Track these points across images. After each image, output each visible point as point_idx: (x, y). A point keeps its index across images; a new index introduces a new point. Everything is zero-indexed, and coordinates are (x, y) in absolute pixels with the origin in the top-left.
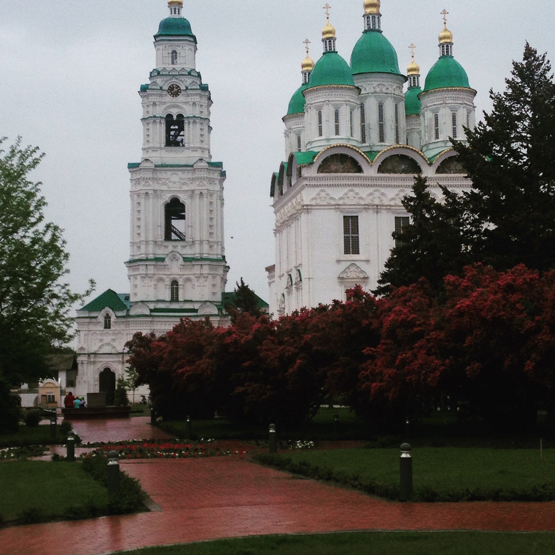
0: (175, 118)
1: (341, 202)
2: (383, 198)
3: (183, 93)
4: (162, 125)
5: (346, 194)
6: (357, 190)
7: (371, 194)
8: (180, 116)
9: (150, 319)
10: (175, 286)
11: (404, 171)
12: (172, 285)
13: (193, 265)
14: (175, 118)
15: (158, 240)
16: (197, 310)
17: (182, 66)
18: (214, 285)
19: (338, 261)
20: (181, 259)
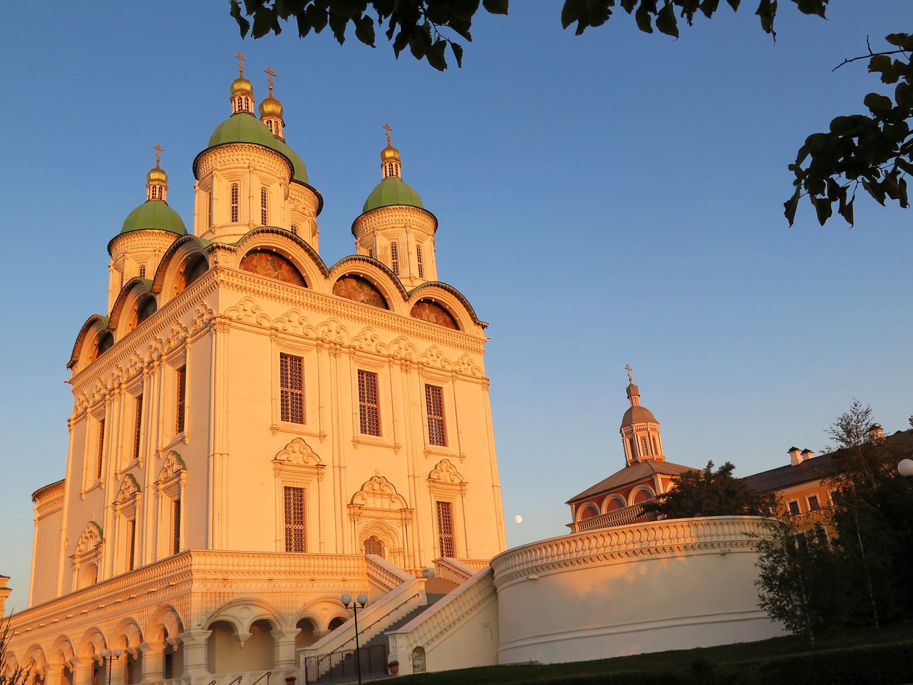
1: (280, 326)
2: (342, 333)
5: (287, 314)
6: (305, 312)
7: (324, 324)
11: (363, 301)
19: (274, 429)
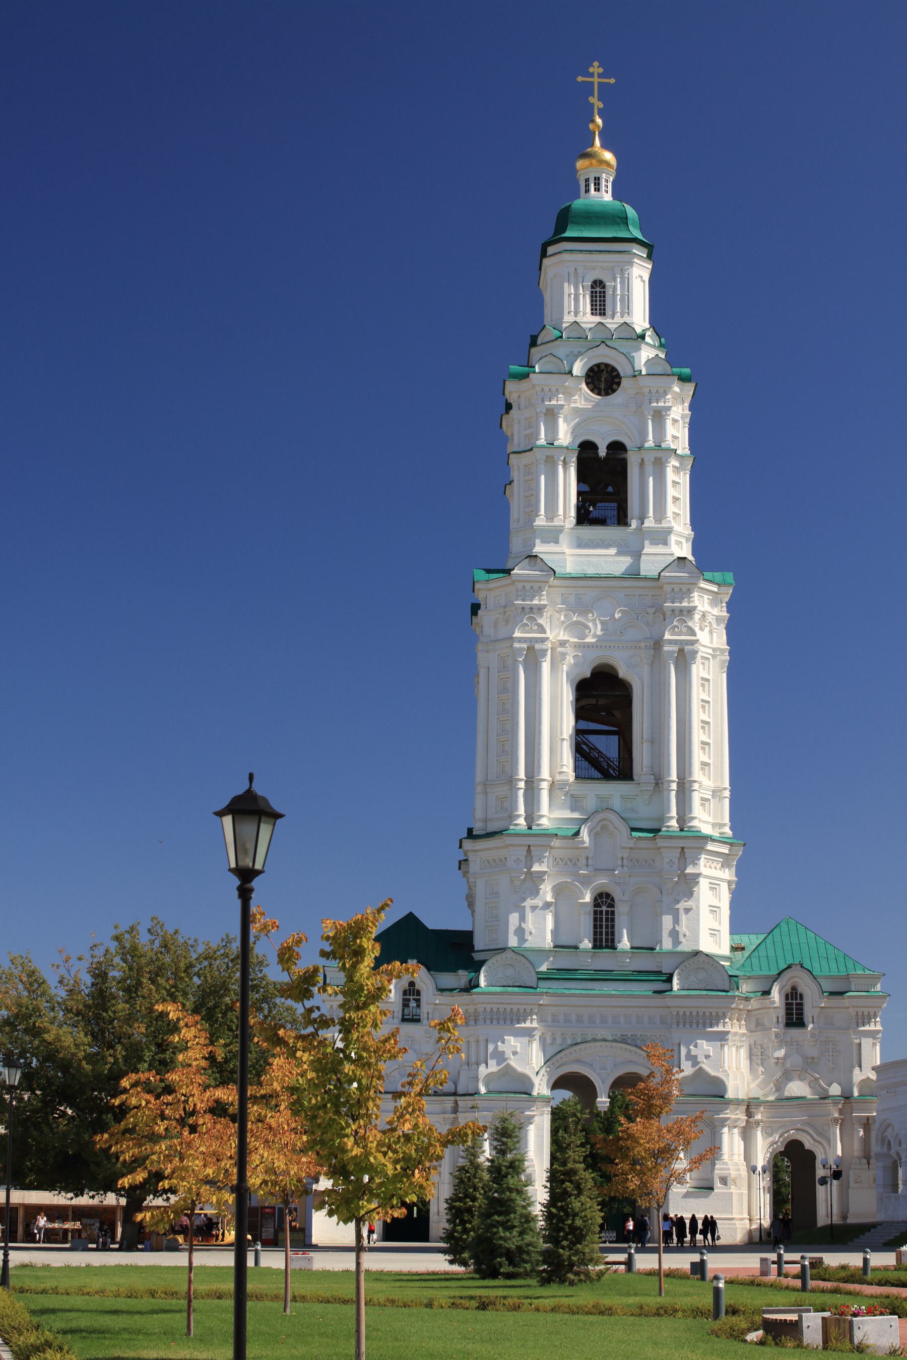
0: (602, 452)
3: (624, 382)
8: (617, 447)
10: (604, 908)
13: (659, 848)
14: (602, 452)
15: (558, 777)
17: (618, 319)
18: (714, 910)
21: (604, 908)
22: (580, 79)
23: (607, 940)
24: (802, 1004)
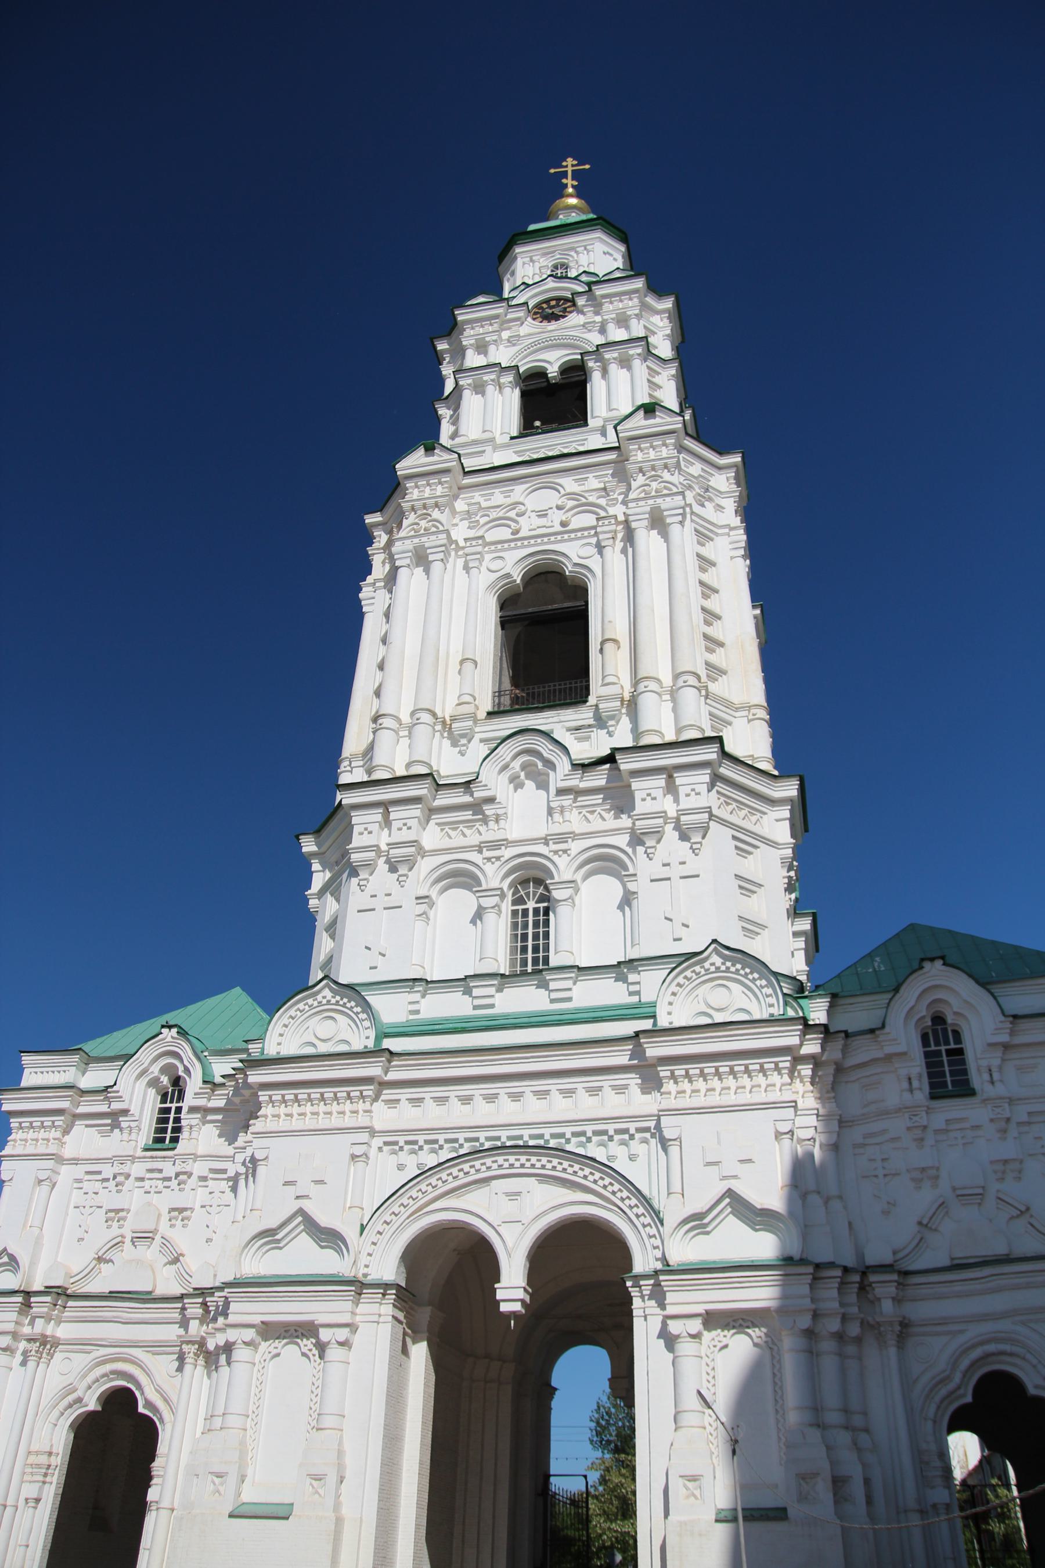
4: (507, 390)
9: (373, 1069)
12: (518, 901)
16: (653, 1005)
20: (563, 766)
21: (531, 905)
22: (552, 171)
23: (535, 961)
24: (960, 1052)
